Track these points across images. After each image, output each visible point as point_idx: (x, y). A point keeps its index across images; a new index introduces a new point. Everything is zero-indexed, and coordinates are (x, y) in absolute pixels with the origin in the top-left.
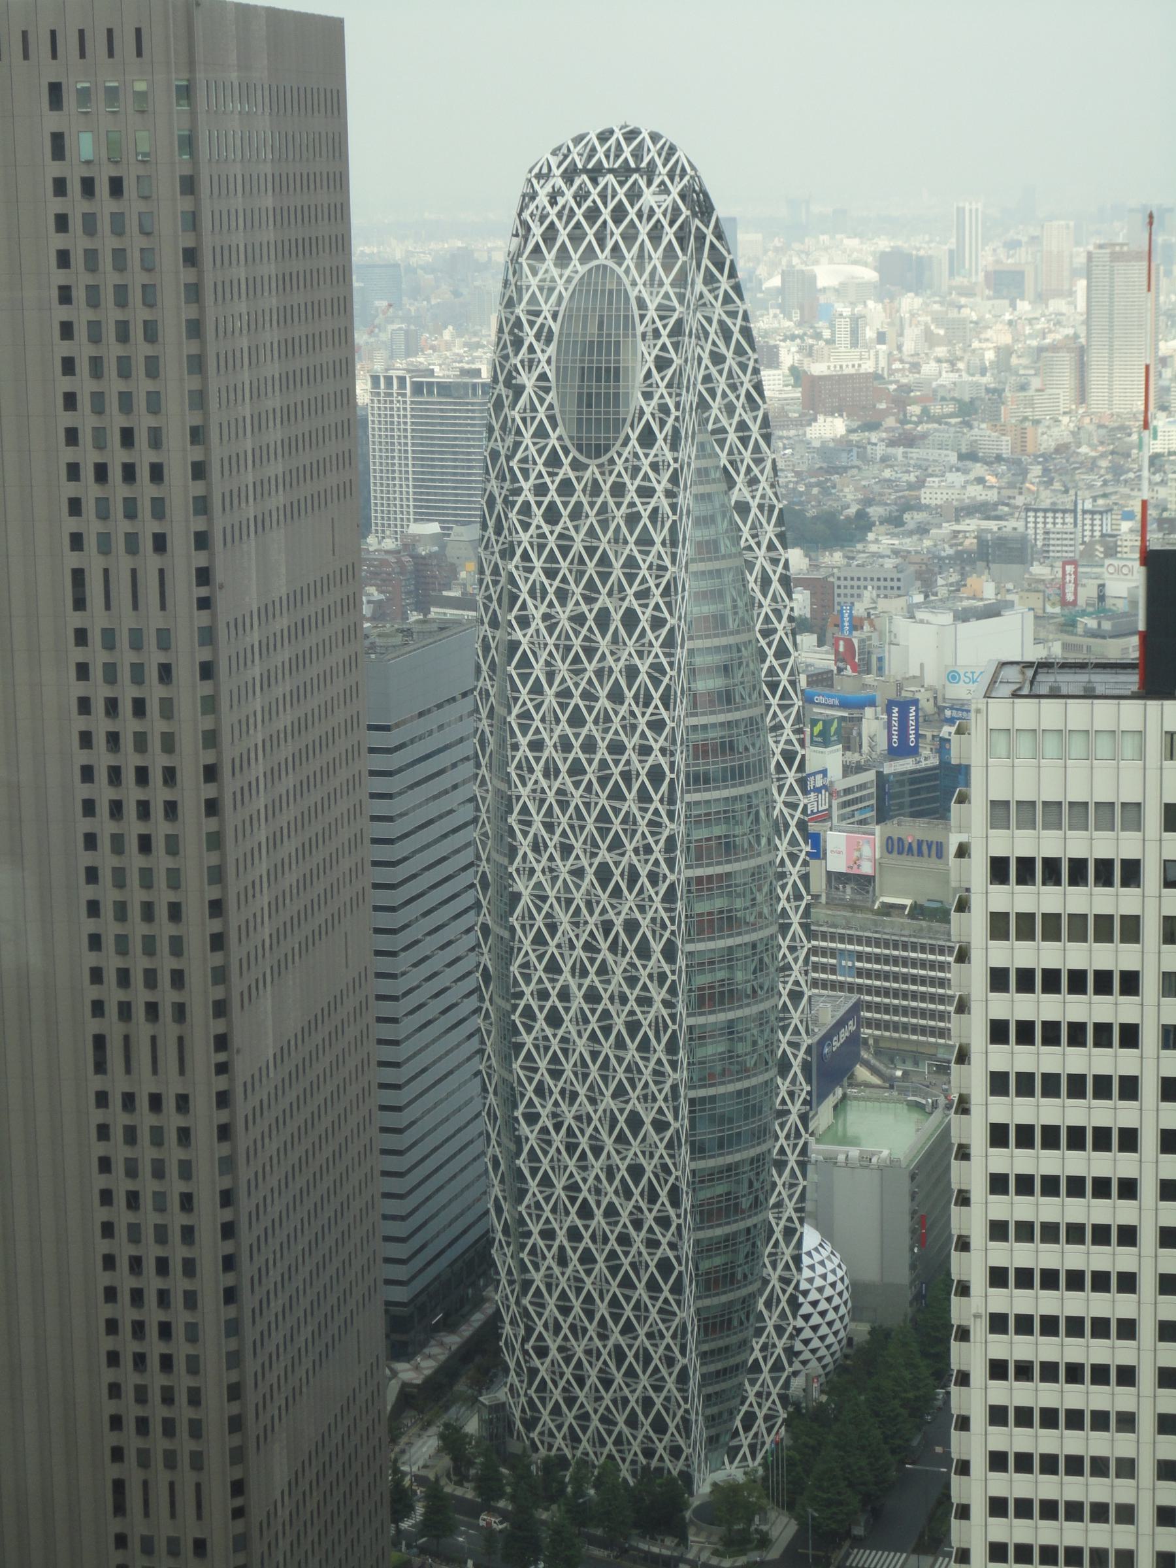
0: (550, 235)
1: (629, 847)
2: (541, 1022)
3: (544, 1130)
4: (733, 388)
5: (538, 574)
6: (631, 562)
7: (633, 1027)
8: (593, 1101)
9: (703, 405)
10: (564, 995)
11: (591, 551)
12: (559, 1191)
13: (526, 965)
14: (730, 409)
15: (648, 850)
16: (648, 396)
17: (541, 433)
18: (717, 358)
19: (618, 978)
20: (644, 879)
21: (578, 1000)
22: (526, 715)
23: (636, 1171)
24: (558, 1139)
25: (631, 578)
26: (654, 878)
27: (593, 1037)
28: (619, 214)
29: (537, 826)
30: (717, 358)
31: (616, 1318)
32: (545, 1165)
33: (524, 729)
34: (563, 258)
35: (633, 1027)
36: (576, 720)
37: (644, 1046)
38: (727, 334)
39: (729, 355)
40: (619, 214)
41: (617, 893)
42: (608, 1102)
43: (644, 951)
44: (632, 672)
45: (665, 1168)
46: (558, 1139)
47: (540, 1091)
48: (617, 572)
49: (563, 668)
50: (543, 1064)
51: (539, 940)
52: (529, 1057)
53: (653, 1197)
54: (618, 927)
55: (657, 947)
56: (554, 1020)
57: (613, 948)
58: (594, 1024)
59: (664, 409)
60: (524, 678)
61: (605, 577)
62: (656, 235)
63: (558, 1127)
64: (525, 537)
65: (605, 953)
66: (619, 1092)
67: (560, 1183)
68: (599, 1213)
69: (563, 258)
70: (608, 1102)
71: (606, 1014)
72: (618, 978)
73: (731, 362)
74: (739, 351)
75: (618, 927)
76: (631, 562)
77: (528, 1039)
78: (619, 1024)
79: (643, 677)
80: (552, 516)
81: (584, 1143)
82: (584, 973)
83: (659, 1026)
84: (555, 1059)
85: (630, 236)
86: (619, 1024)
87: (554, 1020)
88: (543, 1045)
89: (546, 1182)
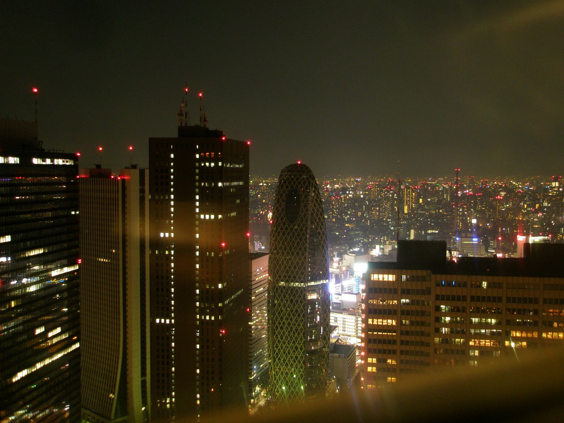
0: (285, 182)
1: (297, 296)
2: (279, 329)
3: (279, 349)
4: (318, 211)
5: (281, 244)
6: (298, 243)
7: (297, 330)
8: (289, 344)
9: (312, 214)
10: (284, 324)
11: (291, 241)
12: (282, 361)
13: (276, 318)
14: (317, 215)
15: (300, 297)
16: (302, 212)
17: (282, 218)
18: (315, 206)
19: (294, 321)
20: (299, 302)
21: (286, 325)
22: (278, 271)
23: (297, 357)
24: (282, 351)
25: (298, 246)
26: (301, 302)
27: (289, 332)
28: (298, 179)
29: (279, 291)
30: (315, 206)
31: (292, 386)
32: (279, 356)
33: (277, 273)
34: (287, 187)
35: (297, 330)
36: (287, 272)
37: (299, 334)
38: (317, 201)
39: (317, 205)
40: (298, 179)
41: (294, 305)
42: (291, 344)
43: (299, 316)
44: (298, 263)
45: (302, 357)
46: (282, 351)
47: (279, 342)
48: (296, 245)
49: (285, 263)
50: (279, 337)
51: (279, 313)
52: (277, 335)
53: (300, 362)
54: (294, 311)
55: (302, 315)
56: (282, 328)
57: (293, 315)
58: (289, 329)
59: (305, 214)
60: (278, 264)
61: (293, 245)
62: (304, 183)
63: (282, 349)
64: (279, 238)
65: (291, 316)
66: (294, 342)
67: (282, 359)
68: (289, 365)
69: (287, 187)
70: (291, 344)
71: (291, 327)
72: (294, 321)
73: (318, 206)
74: (319, 204)
75: (294, 311)
76: (298, 243)
77: (277, 332)
78: (294, 329)
79: (300, 264)
80: (284, 234)
81: (287, 352)
82: (288, 320)
83: (301, 330)
84: (282, 336)
85: (299, 183)
86: (294, 329)
87: (282, 328)
88: (279, 333)
89: (279, 359)
